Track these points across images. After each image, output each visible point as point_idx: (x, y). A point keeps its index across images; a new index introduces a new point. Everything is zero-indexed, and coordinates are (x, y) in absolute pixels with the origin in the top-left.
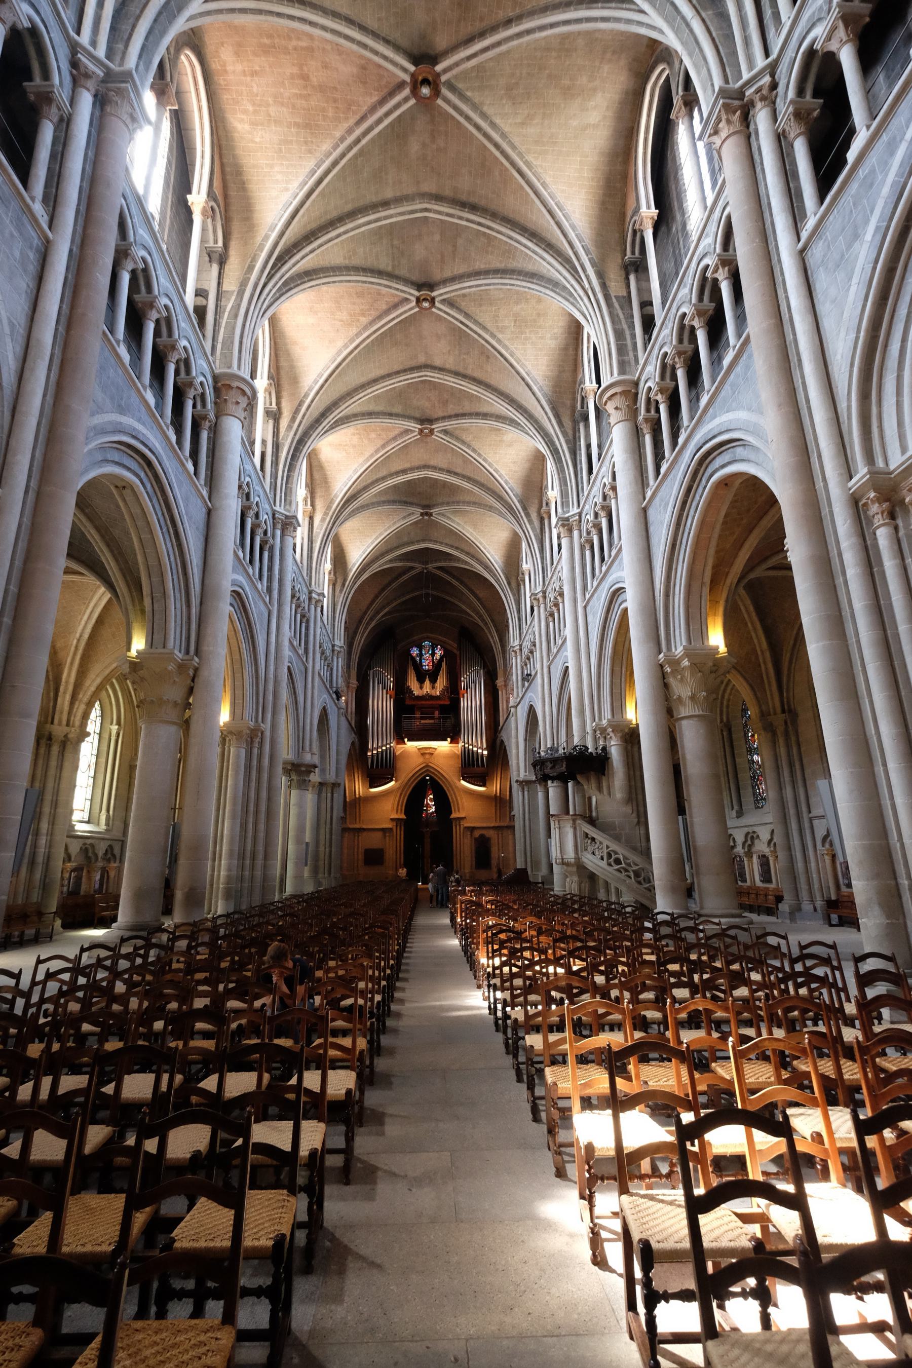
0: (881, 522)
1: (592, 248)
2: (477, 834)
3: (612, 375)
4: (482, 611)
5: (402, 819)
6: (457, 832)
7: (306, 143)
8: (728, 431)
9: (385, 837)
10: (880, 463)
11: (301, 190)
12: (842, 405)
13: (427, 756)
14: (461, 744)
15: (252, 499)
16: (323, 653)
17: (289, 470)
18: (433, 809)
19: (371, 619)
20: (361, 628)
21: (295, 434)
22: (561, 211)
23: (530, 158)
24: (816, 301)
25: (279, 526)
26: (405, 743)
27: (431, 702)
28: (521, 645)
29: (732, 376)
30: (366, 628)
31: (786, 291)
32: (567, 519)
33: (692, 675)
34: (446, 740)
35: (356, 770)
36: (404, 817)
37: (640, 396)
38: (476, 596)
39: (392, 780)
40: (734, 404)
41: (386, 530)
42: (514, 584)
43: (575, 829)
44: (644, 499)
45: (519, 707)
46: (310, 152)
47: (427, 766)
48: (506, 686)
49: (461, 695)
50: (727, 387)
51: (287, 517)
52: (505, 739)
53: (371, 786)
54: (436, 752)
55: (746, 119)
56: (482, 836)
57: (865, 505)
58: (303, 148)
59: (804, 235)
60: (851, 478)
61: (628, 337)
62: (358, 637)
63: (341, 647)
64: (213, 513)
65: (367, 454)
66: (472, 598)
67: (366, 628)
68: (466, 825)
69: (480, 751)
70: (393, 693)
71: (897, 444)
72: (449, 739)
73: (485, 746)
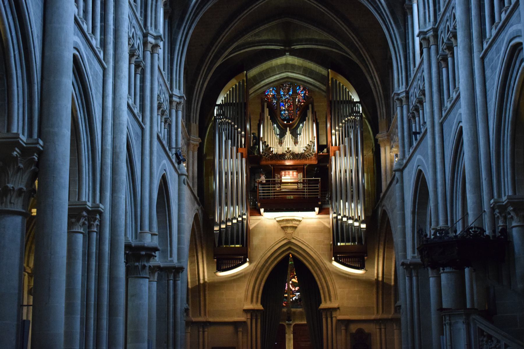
2: (353, 328)
4: (358, 44)
5: (258, 310)
9: (236, 332)
13: (289, 231)
19: (217, 57)
20: (204, 69)
26: (260, 214)
30: (209, 69)
35: (199, 249)
36: (260, 307)
47: (289, 243)
53: (220, 269)
54: (300, 226)
56: (360, 331)
62: (199, 81)
68: (340, 317)
72: (317, 209)
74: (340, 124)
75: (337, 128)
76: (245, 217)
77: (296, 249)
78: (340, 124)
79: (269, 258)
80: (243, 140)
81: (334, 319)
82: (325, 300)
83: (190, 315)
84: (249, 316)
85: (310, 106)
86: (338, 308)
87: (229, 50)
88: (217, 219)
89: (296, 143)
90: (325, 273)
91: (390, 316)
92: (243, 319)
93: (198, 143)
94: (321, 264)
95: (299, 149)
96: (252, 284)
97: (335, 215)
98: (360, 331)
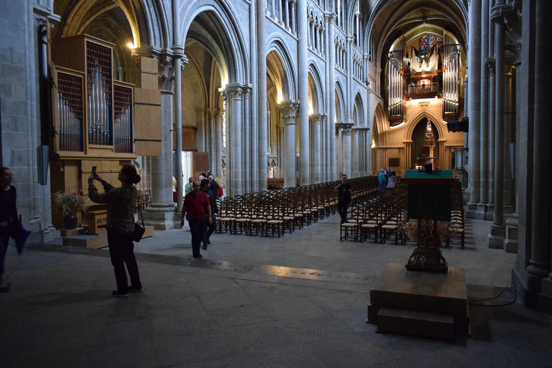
9: (400, 152)
13: (424, 107)
19: (388, 31)
26: (410, 100)
30: (385, 37)
35: (382, 117)
36: (411, 141)
47: (424, 112)
49: (443, 71)
54: (430, 104)
62: (380, 43)
68: (447, 145)
72: (436, 97)
73: (457, 100)
74: (448, 56)
75: (447, 58)
76: (402, 103)
77: (427, 115)
78: (448, 56)
79: (415, 119)
80: (402, 67)
81: (444, 146)
82: (441, 137)
83: (379, 145)
84: (405, 145)
85: (435, 48)
86: (446, 141)
87: (395, 26)
88: (390, 104)
89: (428, 66)
90: (441, 126)
93: (380, 71)
94: (438, 121)
95: (429, 69)
96: (407, 131)
97: (444, 100)
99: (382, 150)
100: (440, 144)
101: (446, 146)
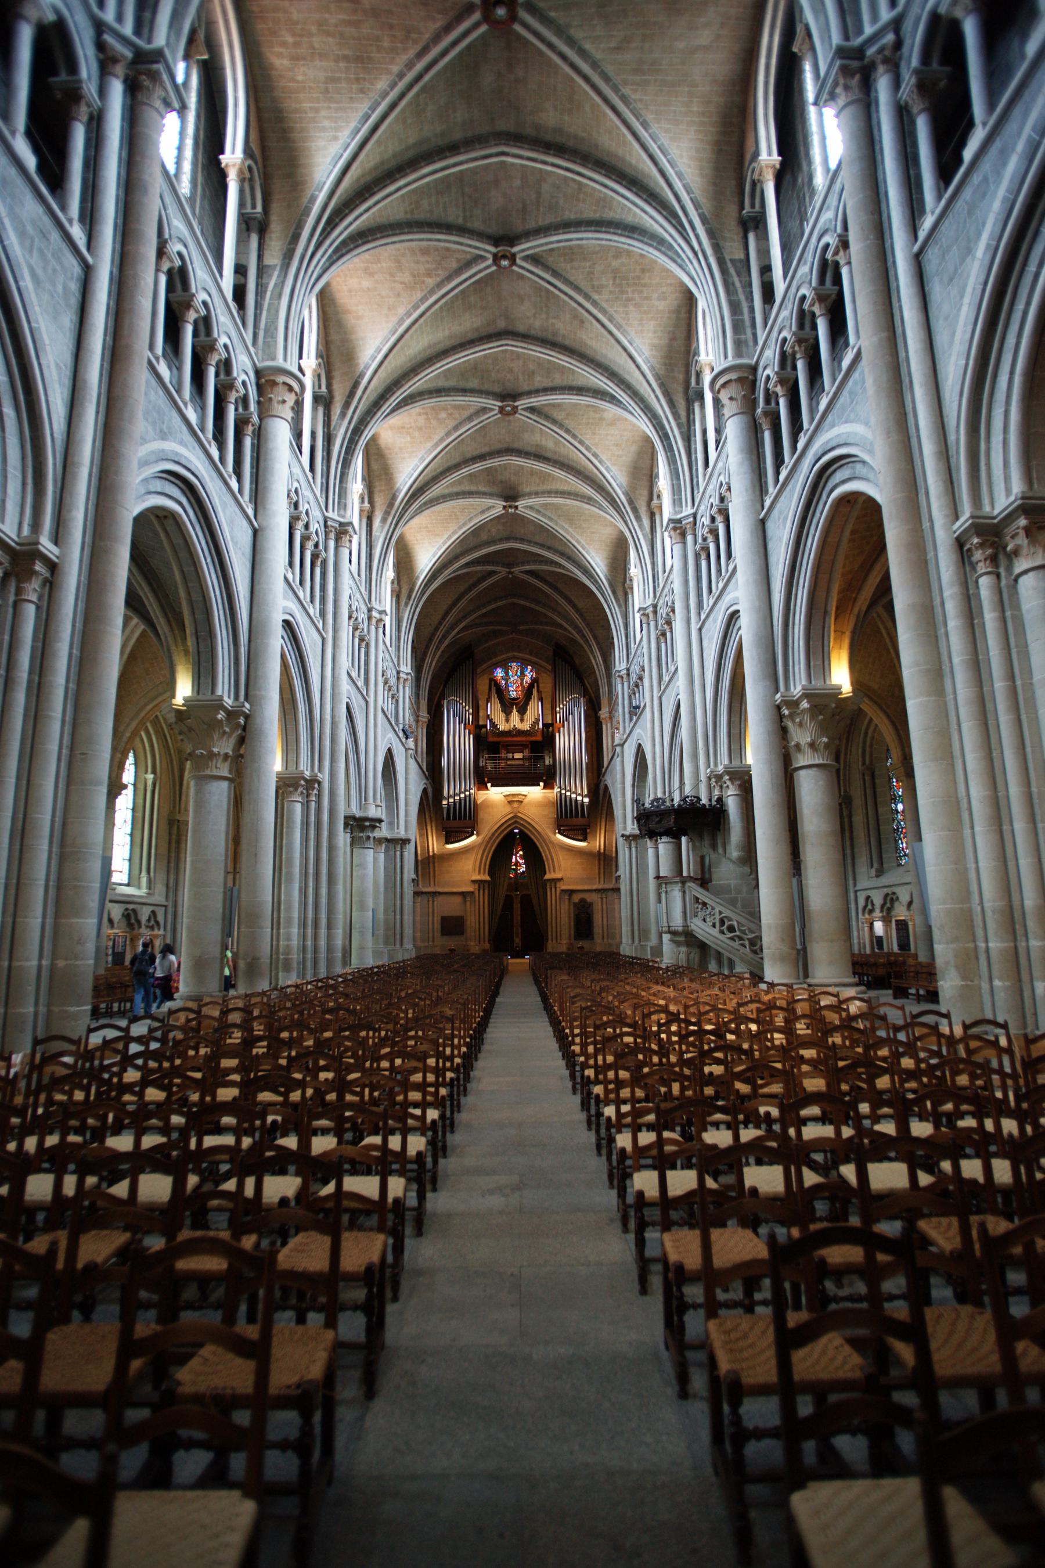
0: (984, 571)
1: (702, 200)
2: (576, 898)
3: (726, 357)
5: (485, 881)
6: (552, 897)
7: (358, 80)
8: (846, 444)
9: (465, 901)
10: (987, 508)
11: (353, 139)
12: (952, 438)
13: (515, 805)
14: (556, 790)
15: (311, 526)
16: (386, 683)
17: (343, 467)
18: (523, 869)
19: (444, 637)
20: (433, 647)
21: (350, 423)
22: (665, 156)
23: (626, 91)
24: (930, 315)
25: (332, 536)
26: (487, 789)
27: (518, 739)
28: (628, 670)
29: (850, 383)
30: (438, 648)
31: (899, 300)
32: (679, 521)
33: (813, 717)
34: (539, 785)
37: (758, 383)
38: (574, 606)
39: (472, 834)
40: (852, 416)
41: (460, 528)
42: (620, 594)
43: (684, 892)
44: (763, 509)
45: (626, 746)
46: (362, 91)
47: (515, 816)
48: (611, 718)
50: (845, 392)
51: (341, 524)
52: (609, 783)
53: (449, 841)
54: (526, 801)
55: (867, 85)
57: (969, 550)
58: (354, 87)
59: (922, 235)
60: (957, 518)
61: (746, 310)
62: (428, 660)
63: (407, 674)
64: (259, 534)
65: (436, 438)
66: (569, 608)
67: (438, 648)
69: (579, 798)
70: (472, 728)
71: (1002, 485)
72: (542, 784)
73: (585, 792)
79: (496, 831)
87: (456, 631)
88: (445, 794)
91: (611, 886)
92: (470, 889)
98: (583, 901)
99: (425, 897)
100: (548, 887)
101: (563, 890)
